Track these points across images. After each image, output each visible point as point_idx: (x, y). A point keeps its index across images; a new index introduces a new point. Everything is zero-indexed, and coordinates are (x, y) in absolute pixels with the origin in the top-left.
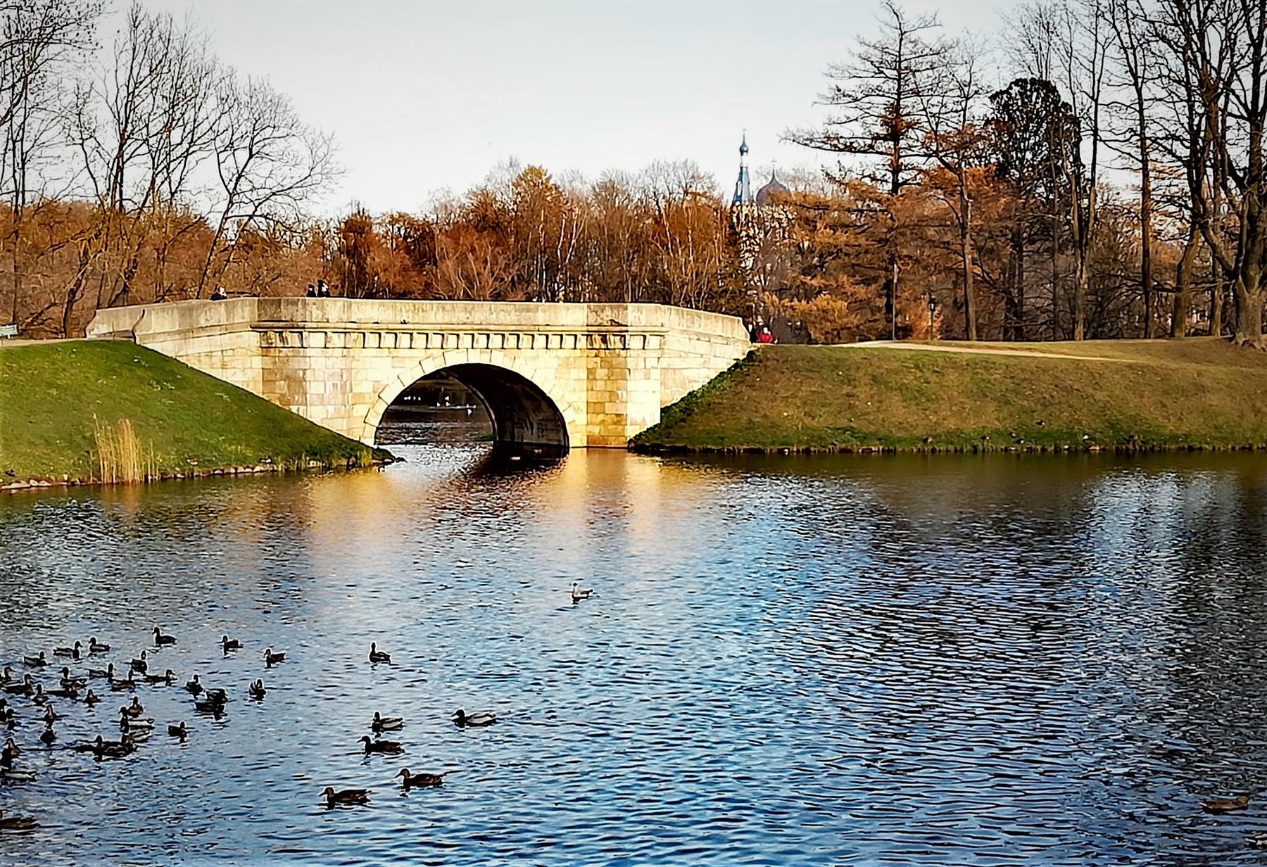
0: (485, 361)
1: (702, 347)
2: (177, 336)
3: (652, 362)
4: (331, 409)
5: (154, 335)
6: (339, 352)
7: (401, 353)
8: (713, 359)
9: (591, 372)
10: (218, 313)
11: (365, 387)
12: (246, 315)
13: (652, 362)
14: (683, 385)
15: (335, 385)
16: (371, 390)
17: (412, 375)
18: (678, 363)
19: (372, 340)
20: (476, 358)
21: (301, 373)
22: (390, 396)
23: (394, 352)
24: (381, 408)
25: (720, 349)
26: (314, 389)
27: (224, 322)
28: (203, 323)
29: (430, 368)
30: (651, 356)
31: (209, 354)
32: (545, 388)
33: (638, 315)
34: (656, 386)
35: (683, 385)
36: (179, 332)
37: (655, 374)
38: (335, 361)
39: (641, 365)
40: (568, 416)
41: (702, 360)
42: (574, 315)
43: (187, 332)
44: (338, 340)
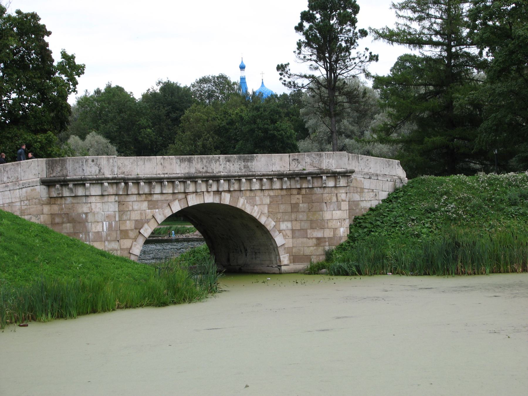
0: (217, 201)
3: (343, 196)
6: (112, 199)
7: (155, 197)
8: (381, 193)
9: (295, 207)
11: (129, 225)
13: (343, 196)
15: (110, 225)
16: (133, 227)
17: (162, 214)
18: (357, 197)
19: (132, 189)
20: (209, 199)
21: (84, 216)
22: (147, 231)
23: (150, 198)
31: (11, 204)
32: (263, 220)
37: (345, 206)
38: (111, 207)
39: (334, 199)
40: (279, 240)
41: (372, 194)
44: (112, 190)
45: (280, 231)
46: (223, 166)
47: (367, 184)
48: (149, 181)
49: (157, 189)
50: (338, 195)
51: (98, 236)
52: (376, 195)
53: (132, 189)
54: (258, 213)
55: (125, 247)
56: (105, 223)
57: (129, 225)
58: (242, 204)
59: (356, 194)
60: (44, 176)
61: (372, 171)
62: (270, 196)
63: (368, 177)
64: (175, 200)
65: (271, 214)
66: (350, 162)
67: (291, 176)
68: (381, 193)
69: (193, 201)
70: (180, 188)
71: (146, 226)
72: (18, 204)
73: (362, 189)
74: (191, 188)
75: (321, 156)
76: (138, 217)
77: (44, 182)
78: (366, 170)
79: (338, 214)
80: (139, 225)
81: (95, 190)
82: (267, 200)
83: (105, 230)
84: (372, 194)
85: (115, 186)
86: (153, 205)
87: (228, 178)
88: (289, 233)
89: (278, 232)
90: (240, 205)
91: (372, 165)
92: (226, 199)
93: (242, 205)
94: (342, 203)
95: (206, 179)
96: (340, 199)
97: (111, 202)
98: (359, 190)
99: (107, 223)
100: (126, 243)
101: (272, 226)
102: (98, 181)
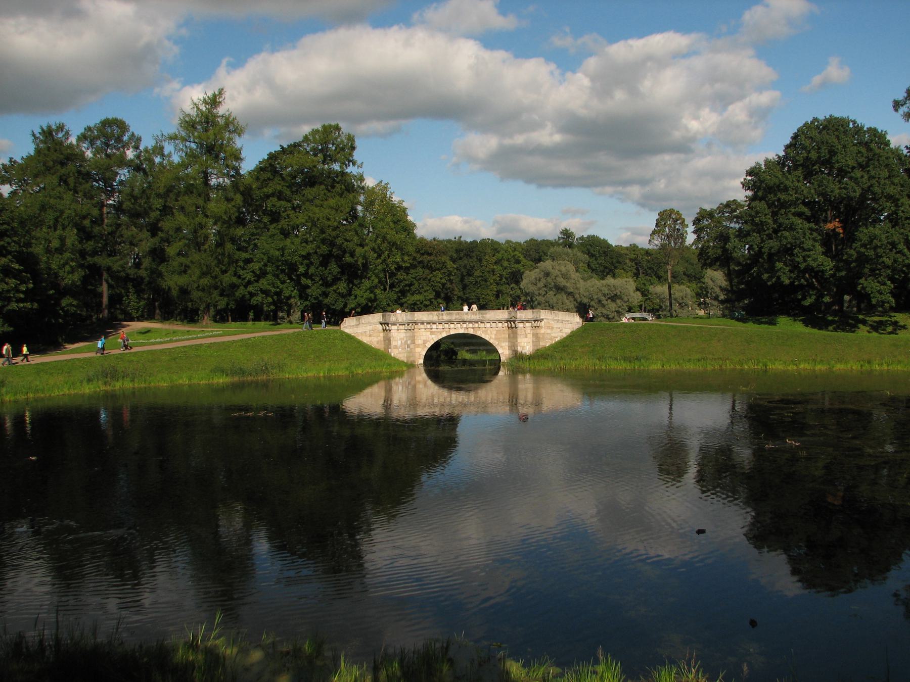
1: (560, 325)
10: (366, 318)
14: (551, 339)
18: (549, 331)
20: (462, 331)
22: (429, 345)
26: (393, 343)
34: (530, 340)
35: (551, 339)
37: (530, 336)
42: (503, 314)
47: (555, 325)
49: (434, 326)
51: (396, 347)
58: (478, 334)
65: (496, 339)
67: (507, 321)
69: (452, 332)
73: (552, 328)
74: (452, 326)
77: (381, 324)
80: (425, 342)
81: (394, 328)
86: (432, 333)
92: (471, 332)
95: (458, 323)
100: (418, 350)
102: (394, 324)
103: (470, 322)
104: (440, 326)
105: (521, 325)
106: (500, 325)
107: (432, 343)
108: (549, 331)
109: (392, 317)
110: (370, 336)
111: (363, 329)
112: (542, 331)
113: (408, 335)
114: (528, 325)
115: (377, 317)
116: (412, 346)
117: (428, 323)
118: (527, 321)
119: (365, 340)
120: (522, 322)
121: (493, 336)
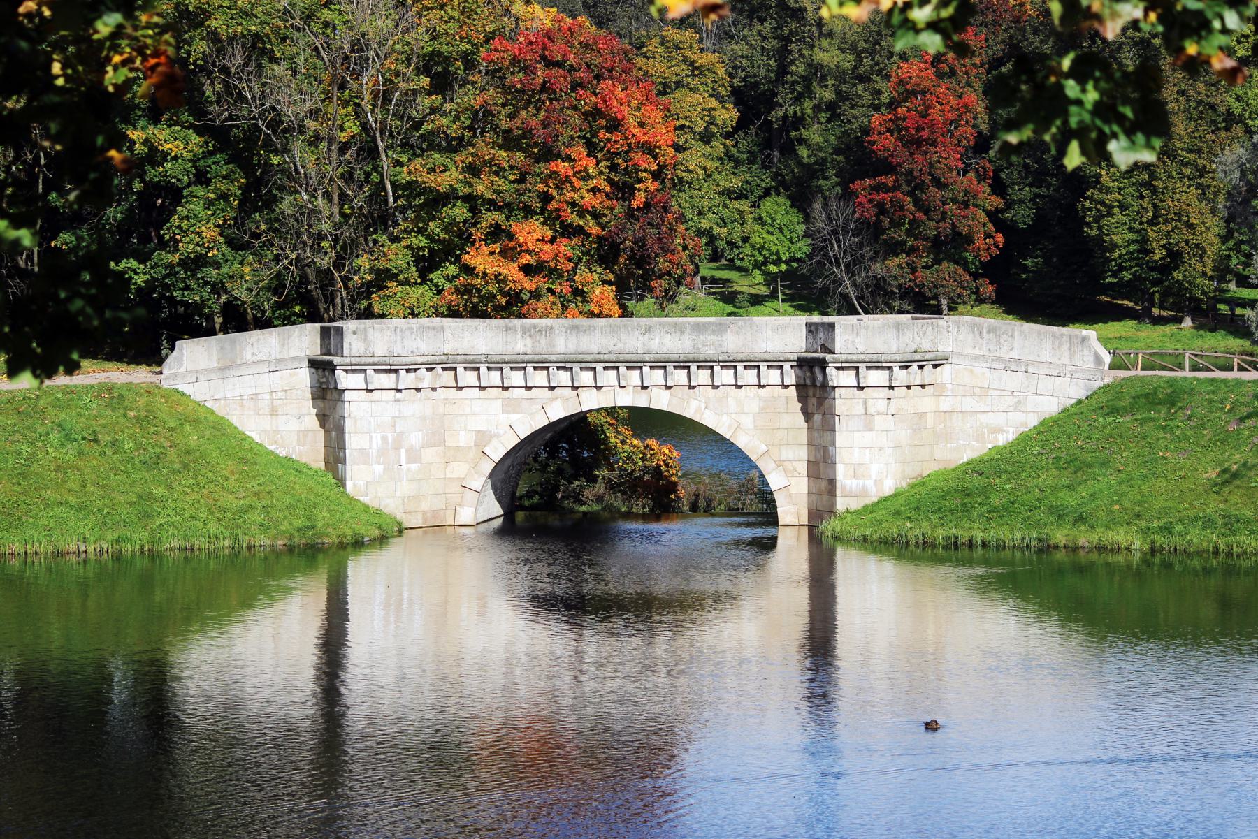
1: (1013, 381)
2: (213, 376)
3: (881, 405)
4: (379, 469)
5: (184, 375)
8: (1032, 398)
11: (465, 439)
12: (305, 346)
15: (384, 438)
17: (529, 421)
18: (969, 404)
20: (625, 399)
24: (488, 467)
25: (1045, 384)
27: (276, 355)
28: (248, 356)
29: (558, 411)
30: (877, 400)
31: (254, 397)
32: (741, 442)
33: (857, 334)
36: (221, 369)
39: (859, 409)
41: (1010, 401)
43: (227, 368)
44: (387, 380)
45: (779, 464)
46: (657, 340)
48: (496, 365)
49: (516, 378)
50: (870, 403)
52: (1019, 402)
53: (468, 378)
54: (730, 426)
55: (454, 475)
56: (374, 435)
57: (465, 439)
59: (969, 399)
60: (315, 351)
61: (1014, 355)
62: (760, 398)
63: (1002, 366)
64: (555, 399)
66: (961, 337)
68: (1032, 398)
69: (591, 401)
70: (564, 377)
71: (495, 442)
72: (267, 396)
74: (586, 377)
75: (832, 326)
76: (484, 428)
78: (1003, 353)
79: (868, 438)
80: (482, 439)
82: (755, 406)
83: (374, 446)
84: (1010, 401)
85: (393, 375)
86: (510, 407)
87: (659, 364)
88: (803, 468)
89: (773, 465)
90: (689, 413)
91: (1017, 342)
92: (661, 401)
93: (696, 412)
94: (877, 417)
96: (871, 410)
97: (387, 402)
98: (977, 391)
99: (379, 436)
100: (459, 469)
101: (760, 452)
103: (659, 364)
104: (539, 378)
105: (847, 378)
106: (773, 376)
107: (512, 442)
108: (969, 404)
109: (362, 339)
110: (274, 412)
111: (244, 384)
112: (945, 404)
113: (429, 413)
114: (876, 378)
115: (302, 340)
116: (430, 455)
117: (496, 365)
118: (875, 366)
119: (255, 427)
120: (853, 366)
121: (747, 422)
